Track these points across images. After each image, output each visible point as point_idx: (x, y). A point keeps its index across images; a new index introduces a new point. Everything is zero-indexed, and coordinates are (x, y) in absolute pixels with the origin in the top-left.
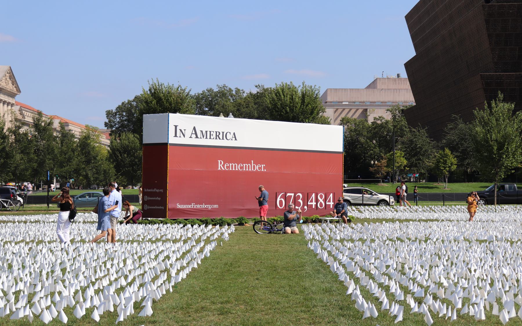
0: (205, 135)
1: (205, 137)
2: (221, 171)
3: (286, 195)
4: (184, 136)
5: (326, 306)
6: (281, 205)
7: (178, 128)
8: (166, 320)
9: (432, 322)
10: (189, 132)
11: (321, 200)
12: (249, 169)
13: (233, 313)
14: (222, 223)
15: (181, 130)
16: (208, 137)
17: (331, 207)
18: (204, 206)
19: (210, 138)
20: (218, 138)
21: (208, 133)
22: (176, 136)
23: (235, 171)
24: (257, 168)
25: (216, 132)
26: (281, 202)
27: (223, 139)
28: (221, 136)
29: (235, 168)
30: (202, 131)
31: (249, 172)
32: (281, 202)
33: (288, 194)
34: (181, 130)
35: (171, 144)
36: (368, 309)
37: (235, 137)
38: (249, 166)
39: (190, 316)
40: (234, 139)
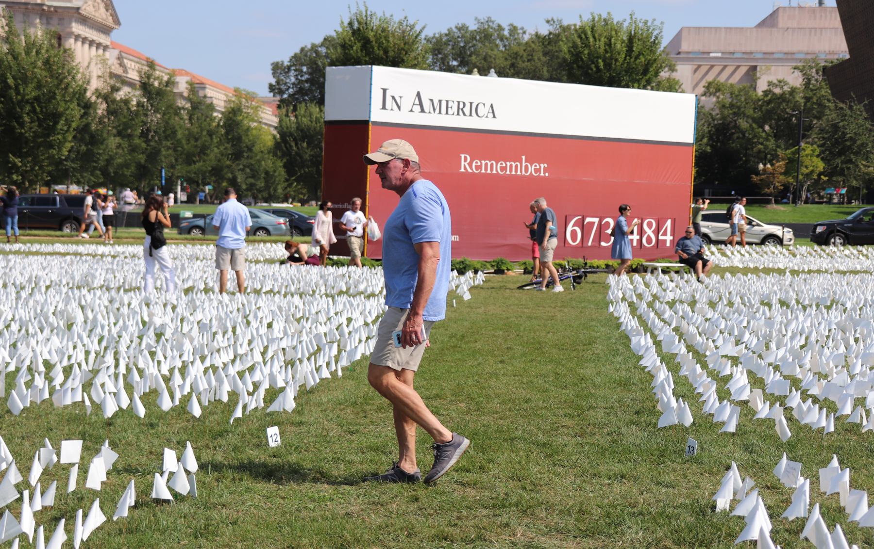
0: (438, 106)
1: (437, 111)
3: (583, 219)
4: (399, 108)
5: (612, 408)
6: (574, 238)
8: (321, 420)
9: (790, 434)
10: (408, 101)
11: (649, 232)
12: (516, 171)
13: (443, 415)
14: (465, 268)
15: (393, 97)
17: (668, 244)
19: (447, 113)
22: (384, 107)
23: (491, 174)
24: (532, 169)
25: (459, 103)
26: (574, 233)
27: (471, 115)
28: (467, 110)
29: (492, 169)
30: (432, 100)
31: (516, 176)
32: (574, 234)
33: (588, 220)
34: (393, 97)
35: (375, 123)
36: (676, 412)
37: (493, 112)
38: (516, 166)
39: (365, 417)
40: (491, 115)
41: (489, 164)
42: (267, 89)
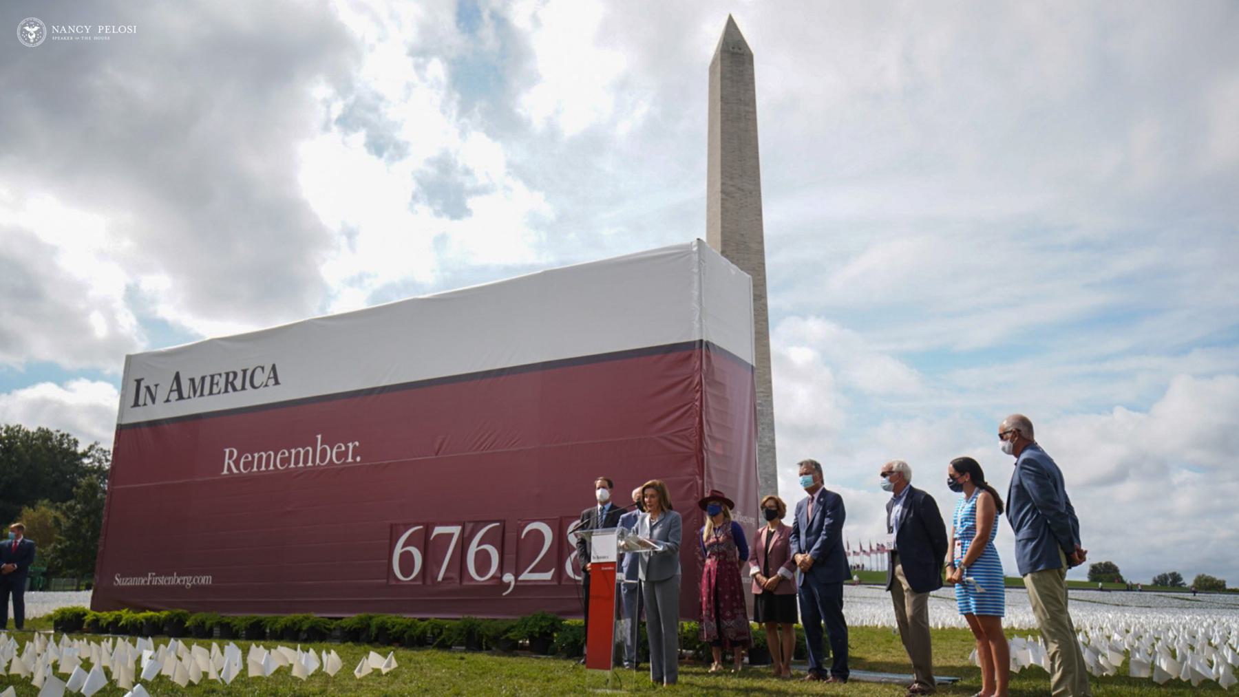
2: (232, 479)
3: (428, 529)
4: (153, 400)
7: (143, 384)
15: (148, 388)
16: (207, 391)
18: (175, 580)
20: (230, 388)
21: (208, 381)
22: (136, 404)
25: (227, 374)
26: (407, 559)
27: (243, 388)
28: (238, 384)
30: (192, 380)
32: (407, 559)
33: (438, 530)
34: (148, 388)
38: (307, 453)
40: (272, 381)
41: (264, 456)
42: (945, 470)
